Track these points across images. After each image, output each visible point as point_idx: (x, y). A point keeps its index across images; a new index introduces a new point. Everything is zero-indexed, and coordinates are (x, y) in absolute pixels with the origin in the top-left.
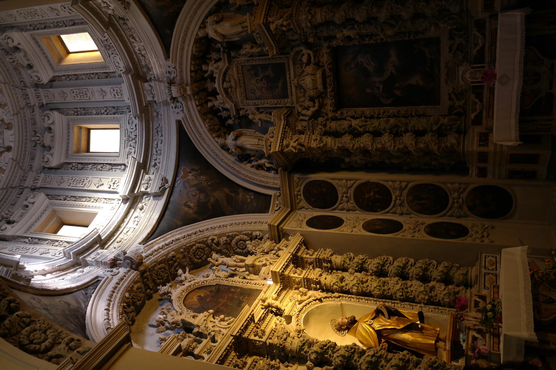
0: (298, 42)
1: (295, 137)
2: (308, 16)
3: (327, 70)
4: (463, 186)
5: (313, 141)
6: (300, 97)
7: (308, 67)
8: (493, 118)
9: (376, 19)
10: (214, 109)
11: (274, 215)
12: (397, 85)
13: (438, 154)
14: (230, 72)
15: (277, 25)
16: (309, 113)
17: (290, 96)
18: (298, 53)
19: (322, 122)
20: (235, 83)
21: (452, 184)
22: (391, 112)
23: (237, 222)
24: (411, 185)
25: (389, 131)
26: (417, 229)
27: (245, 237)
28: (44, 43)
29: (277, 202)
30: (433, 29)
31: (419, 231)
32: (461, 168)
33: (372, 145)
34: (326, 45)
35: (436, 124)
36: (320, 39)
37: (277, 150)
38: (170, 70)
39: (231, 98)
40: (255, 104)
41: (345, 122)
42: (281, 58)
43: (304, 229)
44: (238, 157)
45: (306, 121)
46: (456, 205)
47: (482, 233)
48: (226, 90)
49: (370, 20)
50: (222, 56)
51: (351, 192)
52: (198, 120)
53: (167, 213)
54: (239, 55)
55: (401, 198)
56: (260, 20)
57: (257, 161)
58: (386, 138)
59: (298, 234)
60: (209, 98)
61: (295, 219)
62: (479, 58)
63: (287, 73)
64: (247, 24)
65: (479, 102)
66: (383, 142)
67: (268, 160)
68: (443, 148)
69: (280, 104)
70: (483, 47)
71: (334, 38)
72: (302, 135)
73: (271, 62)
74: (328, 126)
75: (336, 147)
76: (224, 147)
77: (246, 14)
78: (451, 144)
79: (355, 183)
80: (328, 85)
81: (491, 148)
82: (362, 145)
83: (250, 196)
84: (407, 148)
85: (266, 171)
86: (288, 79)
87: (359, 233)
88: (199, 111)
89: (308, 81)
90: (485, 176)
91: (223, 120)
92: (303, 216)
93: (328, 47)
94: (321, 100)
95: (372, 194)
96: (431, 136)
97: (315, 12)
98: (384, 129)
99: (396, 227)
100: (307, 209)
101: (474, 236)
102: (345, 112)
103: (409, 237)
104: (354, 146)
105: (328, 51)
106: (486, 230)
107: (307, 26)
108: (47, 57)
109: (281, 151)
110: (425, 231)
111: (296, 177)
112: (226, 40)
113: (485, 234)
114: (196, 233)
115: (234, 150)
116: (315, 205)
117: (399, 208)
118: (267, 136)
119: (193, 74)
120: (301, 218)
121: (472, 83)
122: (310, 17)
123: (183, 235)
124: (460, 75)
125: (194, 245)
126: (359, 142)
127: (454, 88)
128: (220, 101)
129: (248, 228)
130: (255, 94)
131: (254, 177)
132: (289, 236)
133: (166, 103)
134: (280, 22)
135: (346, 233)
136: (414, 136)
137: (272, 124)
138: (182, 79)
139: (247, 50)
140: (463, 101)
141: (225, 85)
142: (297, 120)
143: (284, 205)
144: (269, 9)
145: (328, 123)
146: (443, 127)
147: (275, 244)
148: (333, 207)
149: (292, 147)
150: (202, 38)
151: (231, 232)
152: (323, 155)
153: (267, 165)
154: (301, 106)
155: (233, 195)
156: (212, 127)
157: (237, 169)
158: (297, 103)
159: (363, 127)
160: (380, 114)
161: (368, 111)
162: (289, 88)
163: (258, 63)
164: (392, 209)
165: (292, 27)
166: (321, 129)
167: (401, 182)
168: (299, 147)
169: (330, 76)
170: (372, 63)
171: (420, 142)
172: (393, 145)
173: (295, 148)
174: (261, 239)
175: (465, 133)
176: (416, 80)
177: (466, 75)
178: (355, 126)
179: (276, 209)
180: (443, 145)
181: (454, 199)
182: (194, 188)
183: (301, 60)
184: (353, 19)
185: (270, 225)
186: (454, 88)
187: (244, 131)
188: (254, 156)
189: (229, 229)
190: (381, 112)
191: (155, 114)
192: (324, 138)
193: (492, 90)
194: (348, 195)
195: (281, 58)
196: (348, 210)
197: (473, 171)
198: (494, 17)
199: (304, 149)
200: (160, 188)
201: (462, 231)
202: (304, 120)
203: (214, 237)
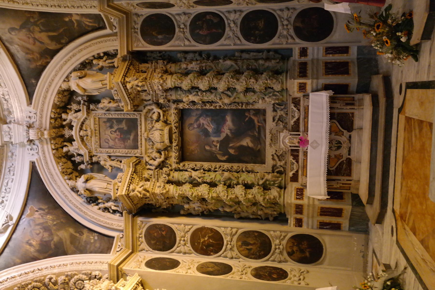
0: (151, 102)
1: (141, 184)
2: (160, 81)
3: (174, 128)
4: (283, 234)
5: (157, 187)
6: (149, 149)
7: (157, 123)
8: (306, 176)
9: (216, 89)
10: (69, 154)
11: (115, 255)
12: (231, 145)
13: (263, 205)
14: (87, 122)
15: (133, 85)
16: (156, 163)
17: (140, 148)
18: (150, 110)
19: (166, 172)
20: (91, 132)
21: (274, 231)
22: (225, 167)
23: (78, 261)
24: (240, 231)
25: (223, 183)
26: (244, 272)
27: (84, 277)
29: (119, 244)
30: (260, 101)
31: (246, 273)
32: (281, 218)
33: (208, 193)
34: (173, 106)
35: (262, 179)
36: (169, 101)
37: (123, 193)
38: (31, 115)
39: (85, 145)
40: (107, 152)
41: (186, 172)
42: (134, 114)
43: (143, 270)
44: (87, 199)
45: (152, 170)
46: (277, 251)
47: (299, 276)
48: (82, 138)
49: (212, 90)
50: (81, 108)
51: (189, 236)
53: (7, 250)
54: (97, 108)
55: (232, 243)
56: (118, 77)
57: (104, 203)
58: (220, 190)
59: (137, 274)
60: (65, 144)
61: (135, 260)
62: (296, 128)
63: (139, 128)
64: (107, 82)
65: (296, 163)
66: (218, 192)
67: (115, 203)
68: (267, 200)
69: (130, 153)
70: (298, 119)
71: (181, 101)
72: (147, 182)
73: (125, 117)
74: (171, 175)
75: (177, 195)
76: (74, 189)
77: (107, 74)
78: (274, 196)
79: (192, 228)
80: (173, 140)
81: (304, 202)
82: (200, 194)
83: (94, 237)
84: (238, 198)
85: (112, 213)
86: (139, 133)
87: (194, 274)
89: (156, 136)
90: (301, 226)
91: (76, 165)
92: (142, 257)
93: (176, 109)
94: (167, 153)
95: (206, 239)
96: (258, 189)
97: (166, 79)
98: (219, 181)
99: (226, 269)
100: (147, 251)
101: (292, 279)
102: (186, 164)
103: (238, 278)
104: (192, 194)
105: (175, 112)
106: (302, 274)
107: (159, 89)
109: (128, 196)
110: (251, 274)
111: (139, 220)
112: (86, 94)
113: (302, 277)
114: (33, 271)
115: (83, 192)
116: (155, 248)
117: (230, 252)
118: (116, 180)
119: (53, 121)
120: (140, 260)
121: (290, 146)
122: (161, 82)
123: (19, 273)
124: (281, 140)
125: (30, 284)
126: (198, 191)
127: (276, 151)
128: (75, 148)
129: (87, 268)
130: (108, 143)
131: (100, 218)
132: (127, 276)
133: (22, 145)
134: (136, 82)
135: (181, 274)
136: (244, 187)
137: (121, 170)
138: (41, 124)
139: (105, 104)
140: (284, 162)
141: (82, 133)
142: (144, 169)
143: (126, 247)
144: (127, 72)
145: (171, 173)
146: (268, 182)
147: (113, 284)
148: (172, 250)
150: (65, 91)
151: (70, 271)
152: (165, 202)
153: (114, 208)
154: (149, 156)
155: (78, 235)
156: (64, 170)
157: (84, 210)
158: (146, 154)
159: (202, 178)
160: (216, 168)
161: (206, 165)
162: (139, 140)
163: (114, 117)
164: (223, 253)
165: (146, 89)
166: (165, 177)
167: (232, 228)
168: (144, 192)
169: (175, 132)
170: (211, 125)
171: (249, 193)
172: (226, 194)
173: (140, 193)
174: (100, 279)
175: (285, 188)
176: (247, 142)
177: (286, 140)
178: (195, 177)
179: (118, 250)
180: (267, 197)
181: (276, 245)
182: (38, 227)
183: (151, 118)
184: (198, 88)
185: (110, 265)
186: (276, 151)
187: (95, 175)
188: (102, 199)
189: (69, 269)
190: (218, 166)
191: (10, 154)
192: (167, 186)
193: (305, 154)
194: (186, 239)
195: (134, 114)
196: (185, 253)
197: (291, 221)
198: (307, 96)
199: (148, 194)
200: (3, 225)
201: (282, 275)
202: (150, 169)
203: (52, 276)
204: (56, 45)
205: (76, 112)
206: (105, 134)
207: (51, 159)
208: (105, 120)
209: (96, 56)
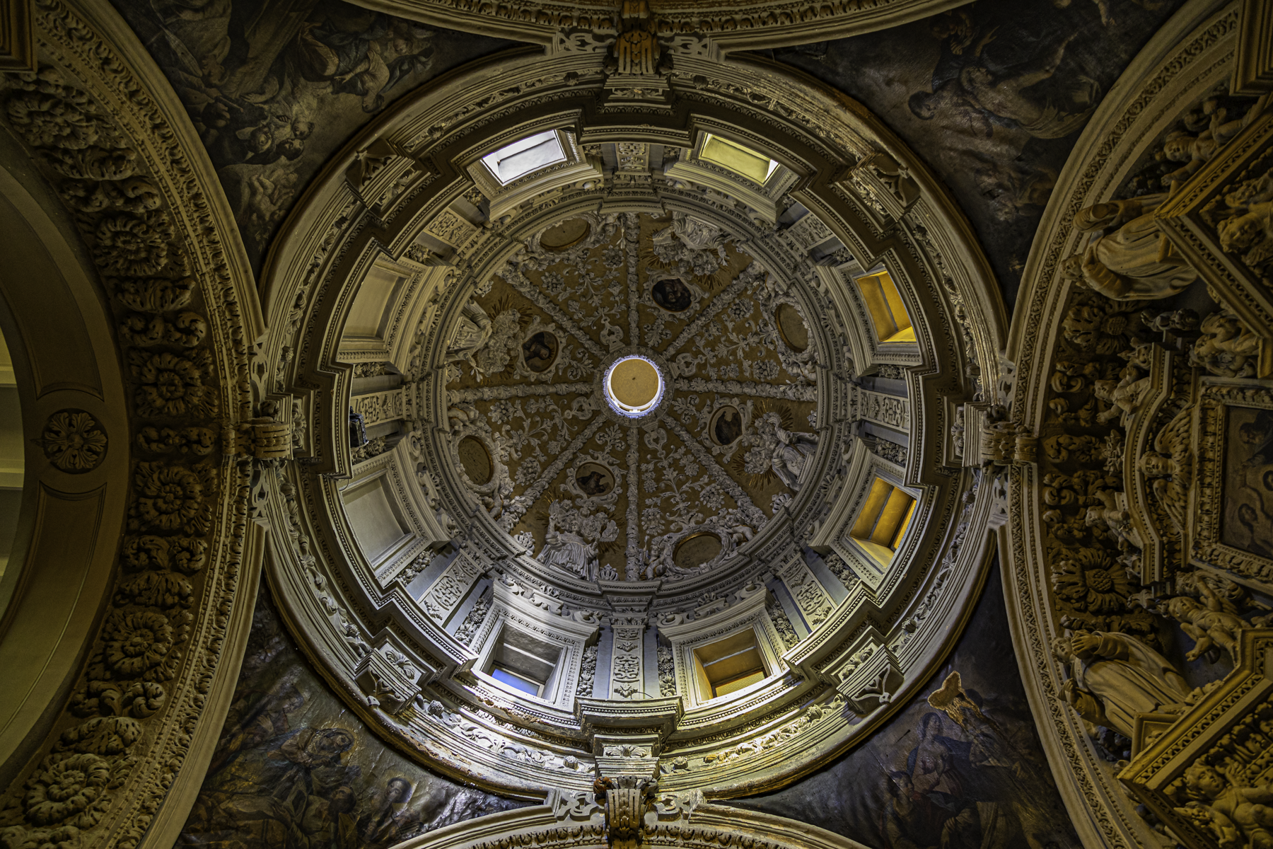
14: (1178, 421)
20: (1188, 462)
28: (864, 290)
37: (1153, 784)
48: (1148, 481)
52: (1034, 551)
53: (840, 768)
88: (1046, 526)
108: (866, 322)
119: (1058, 405)
130: (1251, 528)
139: (1216, 343)
149: (1226, 812)
187: (1138, 648)
200: (864, 692)
204: (1061, 119)
205: (1142, 374)
206: (1244, 485)
207: (1033, 541)
208: (1251, 419)
209: (1189, 120)
